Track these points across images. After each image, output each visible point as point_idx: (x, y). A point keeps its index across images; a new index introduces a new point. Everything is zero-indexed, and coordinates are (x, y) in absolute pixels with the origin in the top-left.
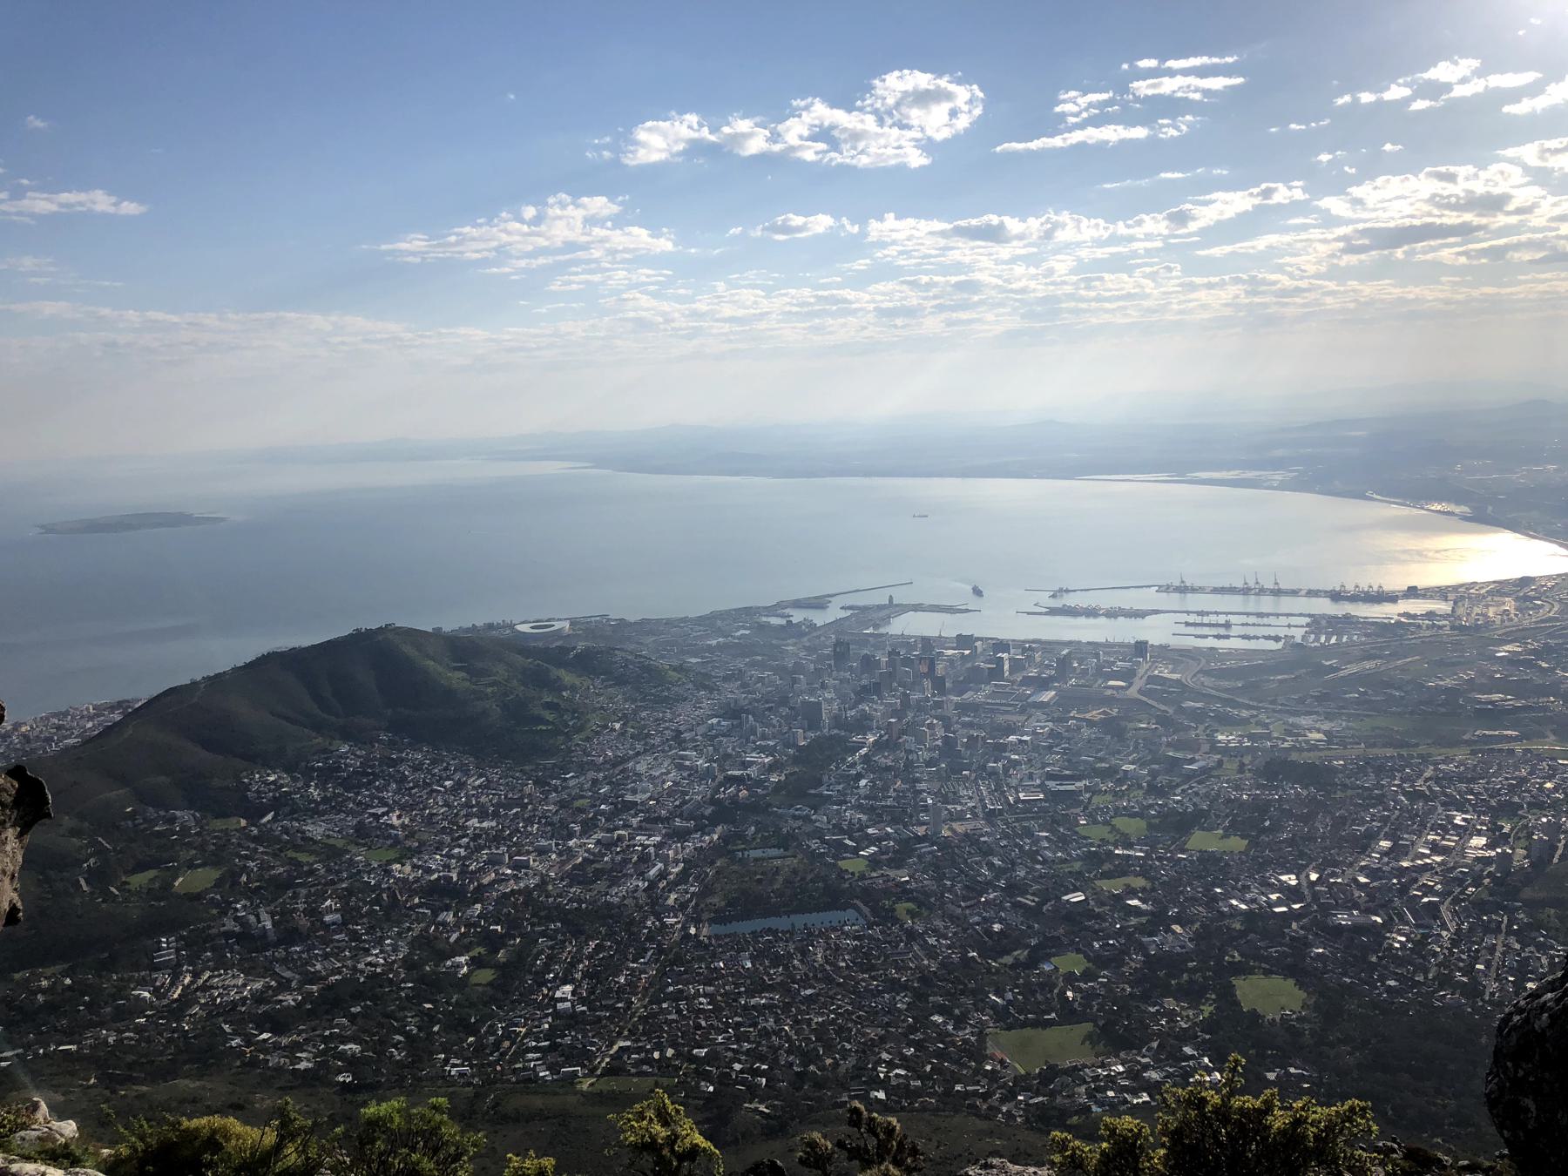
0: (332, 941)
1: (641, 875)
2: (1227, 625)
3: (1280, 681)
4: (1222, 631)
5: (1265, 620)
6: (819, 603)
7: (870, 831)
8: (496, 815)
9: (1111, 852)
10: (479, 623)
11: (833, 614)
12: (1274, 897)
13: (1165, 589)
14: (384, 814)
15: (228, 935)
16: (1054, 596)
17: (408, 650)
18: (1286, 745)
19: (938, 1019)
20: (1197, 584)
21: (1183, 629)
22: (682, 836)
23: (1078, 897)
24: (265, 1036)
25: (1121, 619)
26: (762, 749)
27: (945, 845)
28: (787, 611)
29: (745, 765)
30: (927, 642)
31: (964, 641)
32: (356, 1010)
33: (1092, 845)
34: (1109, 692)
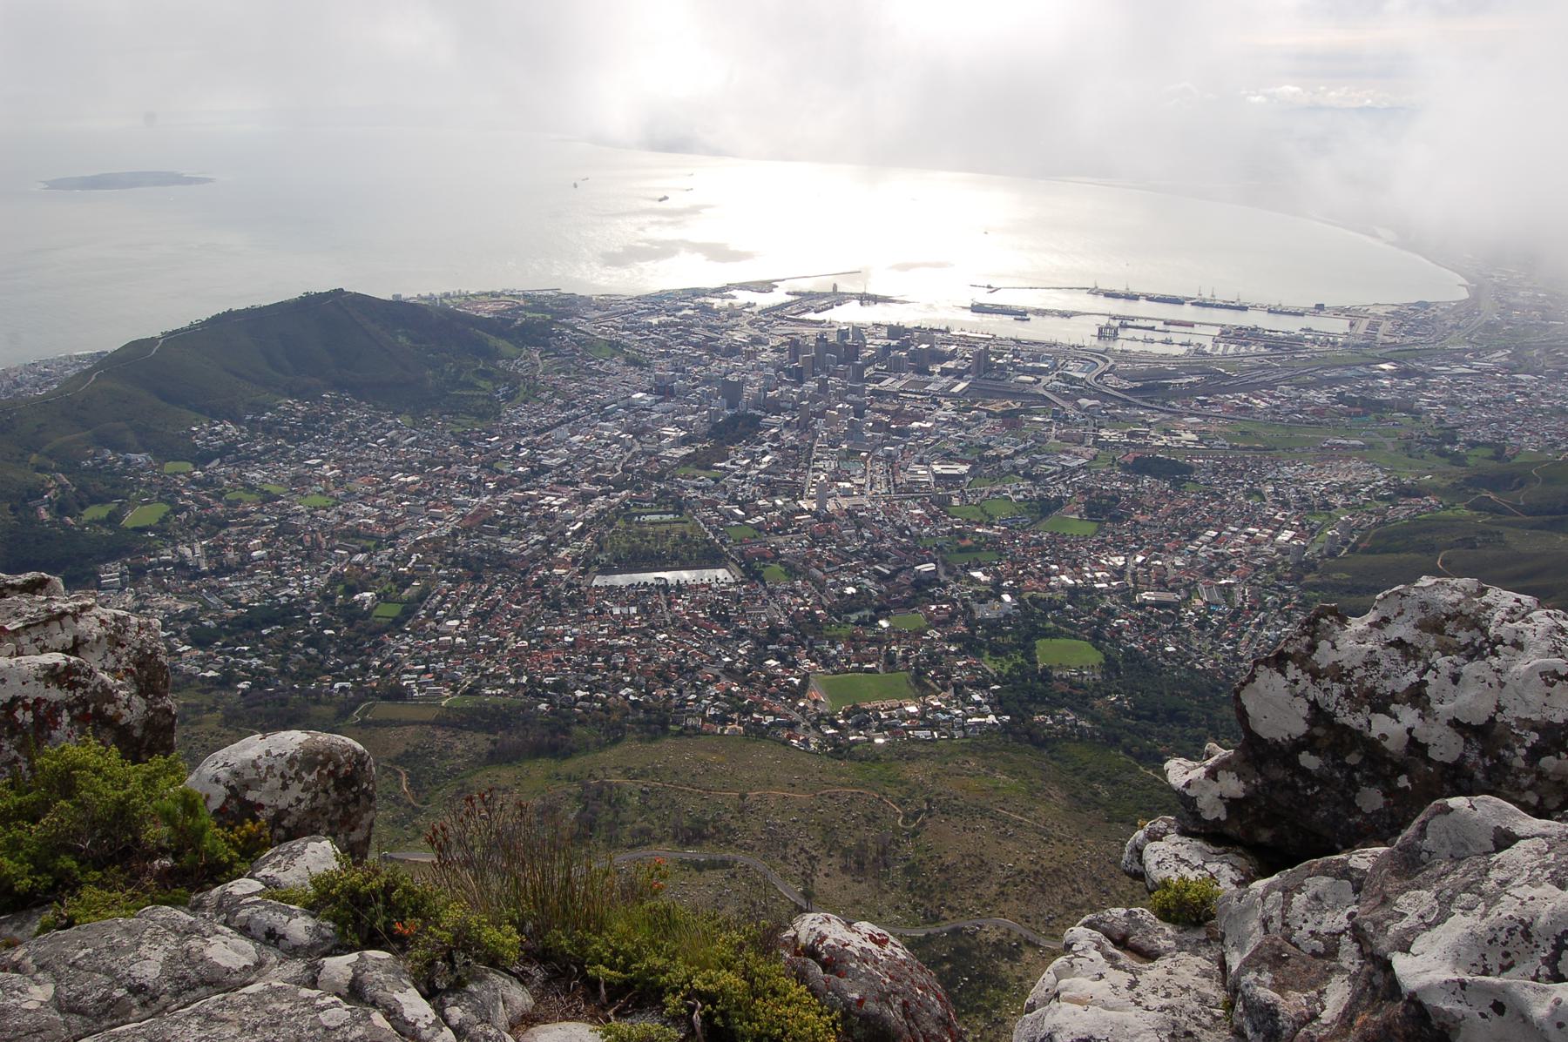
6: (767, 287)
8: (421, 471)
10: (437, 293)
11: (778, 297)
12: (1099, 575)
13: (1095, 292)
15: (167, 564)
19: (772, 662)
24: (186, 648)
26: (678, 425)
27: (829, 518)
28: (734, 293)
29: (661, 437)
30: (858, 331)
31: (895, 331)
32: (265, 632)
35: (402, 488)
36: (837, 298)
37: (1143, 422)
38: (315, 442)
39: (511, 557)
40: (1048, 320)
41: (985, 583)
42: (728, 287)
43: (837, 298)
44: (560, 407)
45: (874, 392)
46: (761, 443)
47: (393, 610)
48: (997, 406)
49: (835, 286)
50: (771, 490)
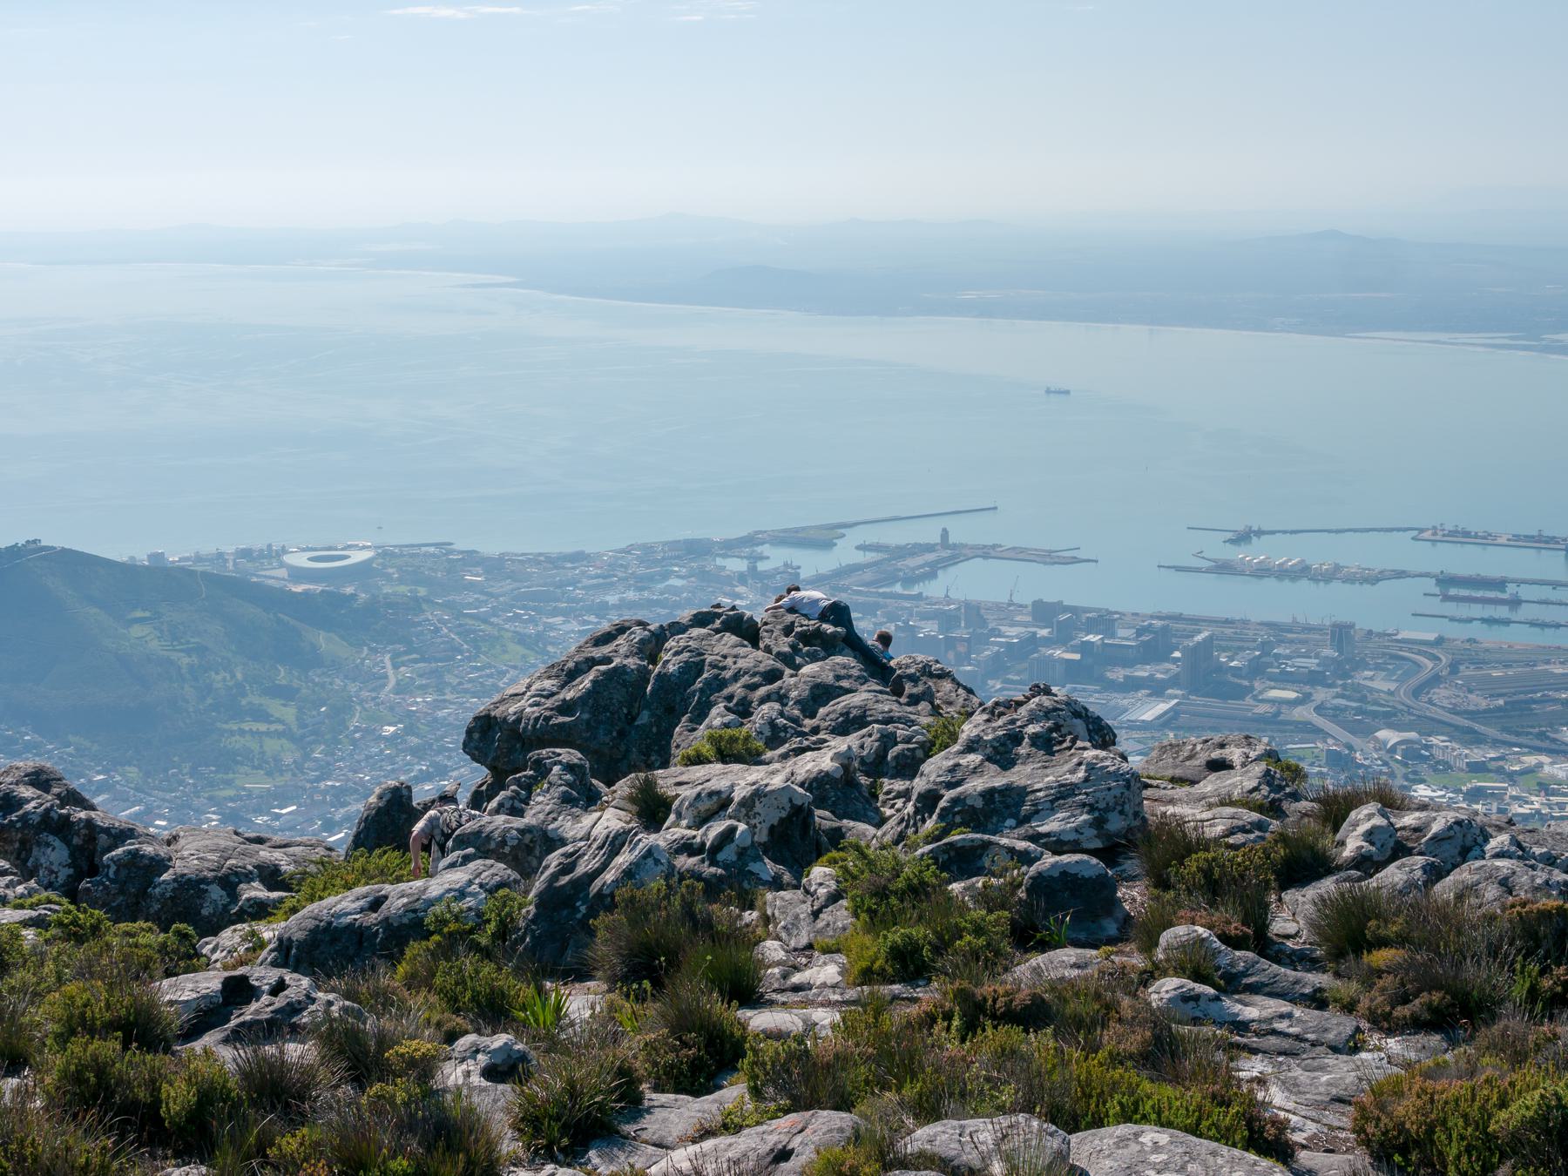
4: (1502, 612)
6: (822, 538)
11: (845, 553)
16: (1231, 541)
18: (1525, 810)
21: (1436, 606)
25: (1304, 583)
30: (974, 612)
31: (1043, 611)
34: (1262, 709)
36: (952, 554)
37: (1500, 771)
42: (751, 540)
43: (952, 554)
49: (945, 533)
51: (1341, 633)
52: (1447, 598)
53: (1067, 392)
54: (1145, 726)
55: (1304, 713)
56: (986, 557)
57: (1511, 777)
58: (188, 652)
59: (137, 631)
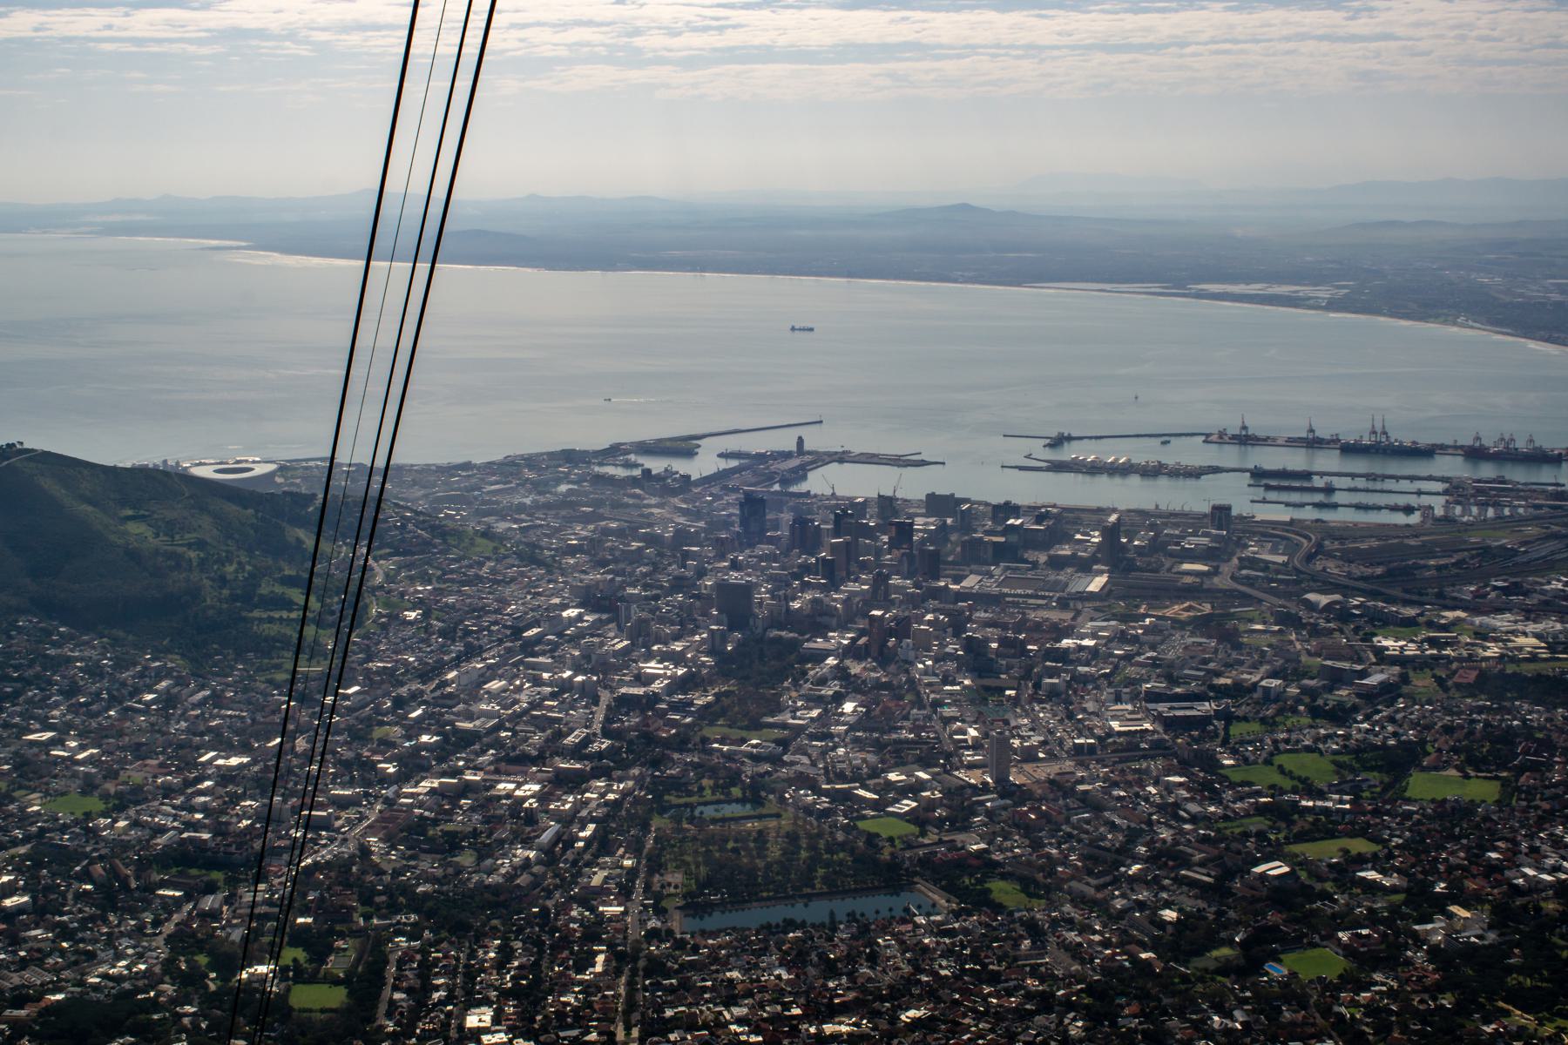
0: (25, 940)
1: (527, 843)
2: (1329, 490)
3: (1439, 568)
4: (1319, 498)
5: (1378, 485)
6: (684, 447)
7: (893, 776)
8: (245, 749)
9: (1295, 804)
14: (52, 743)
16: (1049, 445)
17: (49, 484)
20: (1261, 434)
21: (1260, 493)
22: (573, 782)
23: (1277, 869)
26: (663, 657)
28: (632, 457)
29: (643, 679)
31: (938, 504)
33: (1259, 794)
34: (1189, 580)
35: (226, 777)
38: (30, 701)
39: (495, 889)
40: (1163, 481)
41: (1394, 890)
44: (442, 633)
45: (960, 596)
46: (822, 681)
47: (335, 997)
48: (1176, 610)
49: (800, 441)
50: (898, 755)
51: (1221, 514)
52: (1268, 488)
53: (811, 330)
54: (1092, 596)
55: (1222, 582)
56: (841, 461)
57: (1444, 628)
58: (190, 546)
59: (134, 528)
